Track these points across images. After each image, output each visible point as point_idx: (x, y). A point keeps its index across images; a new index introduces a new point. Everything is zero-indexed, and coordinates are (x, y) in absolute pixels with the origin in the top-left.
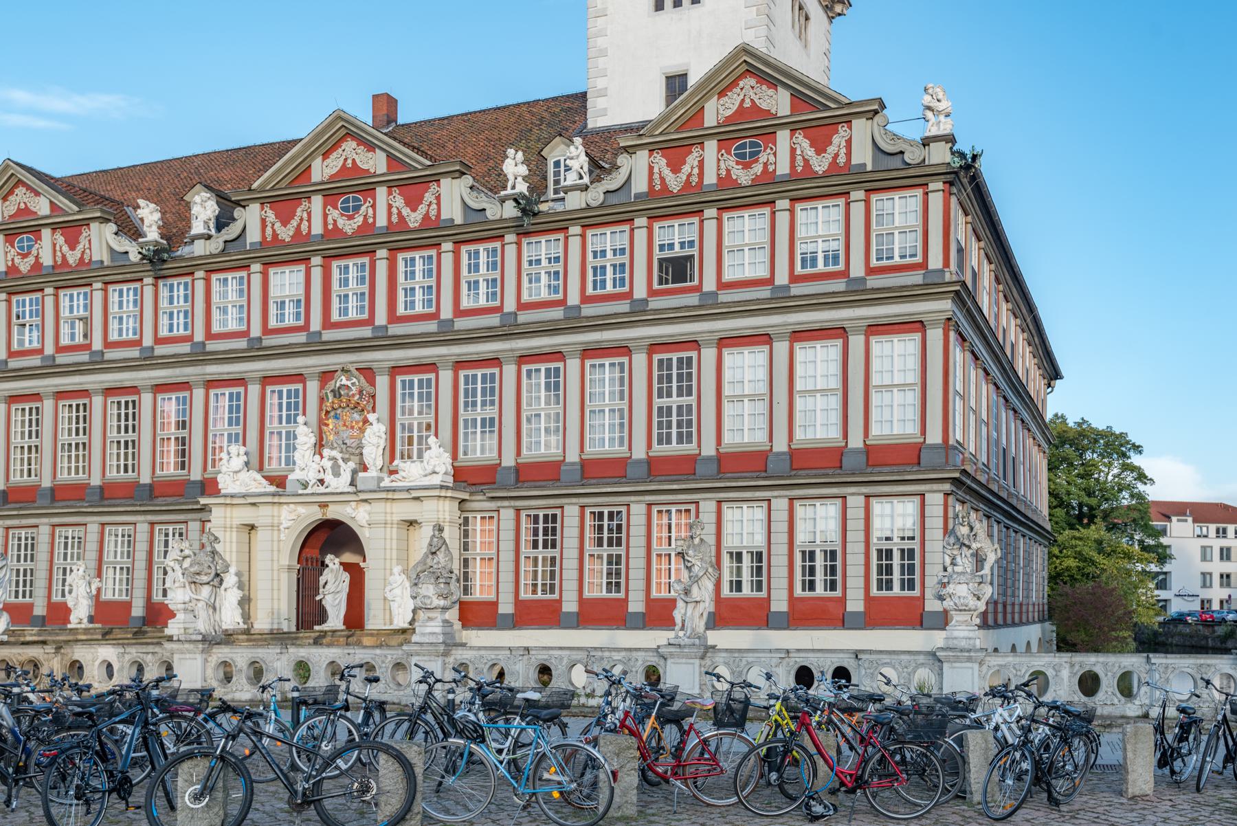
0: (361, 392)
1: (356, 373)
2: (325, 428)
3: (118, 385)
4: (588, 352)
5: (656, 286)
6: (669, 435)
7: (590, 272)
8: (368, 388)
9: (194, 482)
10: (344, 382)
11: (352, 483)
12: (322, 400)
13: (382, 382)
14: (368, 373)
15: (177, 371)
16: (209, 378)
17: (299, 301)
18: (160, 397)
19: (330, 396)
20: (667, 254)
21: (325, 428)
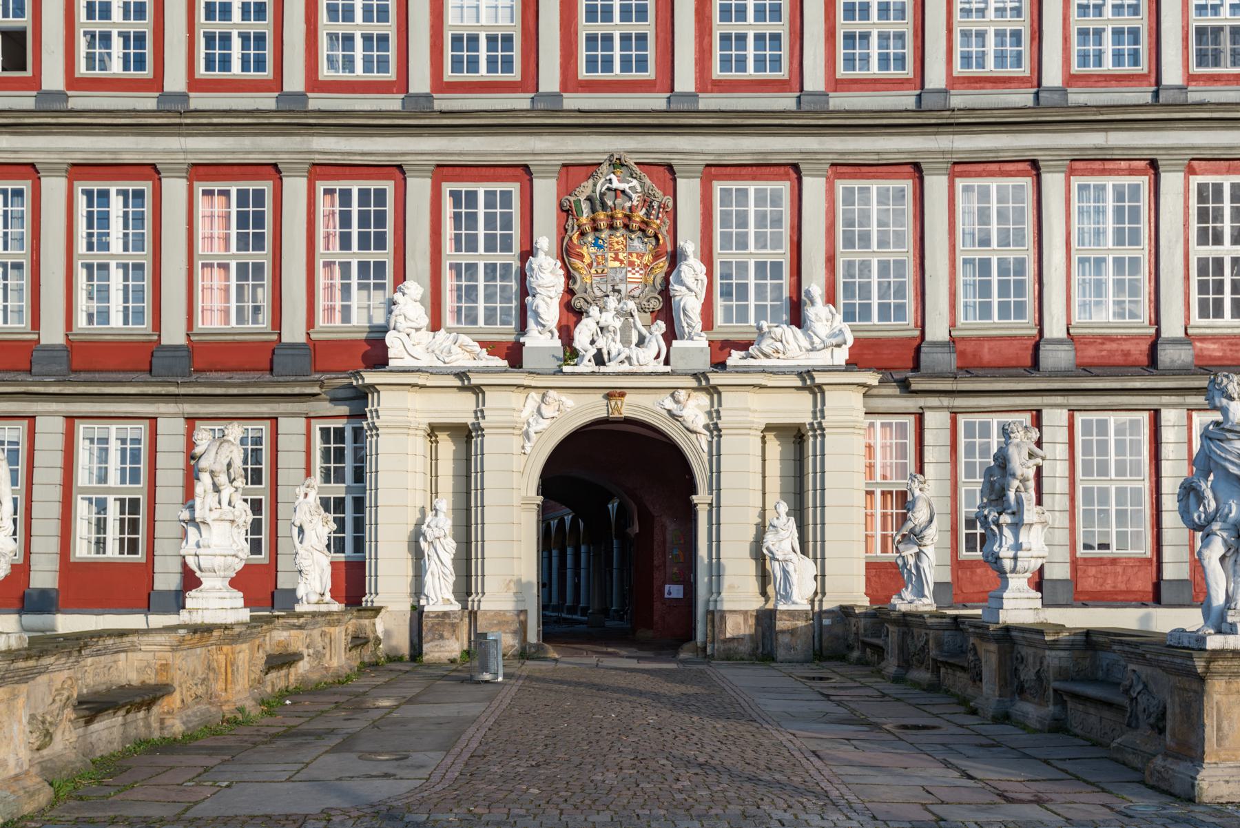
0: (647, 202)
1: (636, 168)
2: (577, 262)
3: (107, 158)
4: (1079, 163)
5: (1195, 70)
6: (1219, 304)
7: (1074, 38)
8: (660, 196)
9: (293, 346)
10: (616, 184)
11: (667, 362)
12: (566, 212)
13: (688, 189)
14: (668, 172)
15: (247, 143)
16: (319, 159)
17: (508, 39)
18: (199, 187)
19: (585, 207)
20: (1209, 21)
21: (577, 262)
